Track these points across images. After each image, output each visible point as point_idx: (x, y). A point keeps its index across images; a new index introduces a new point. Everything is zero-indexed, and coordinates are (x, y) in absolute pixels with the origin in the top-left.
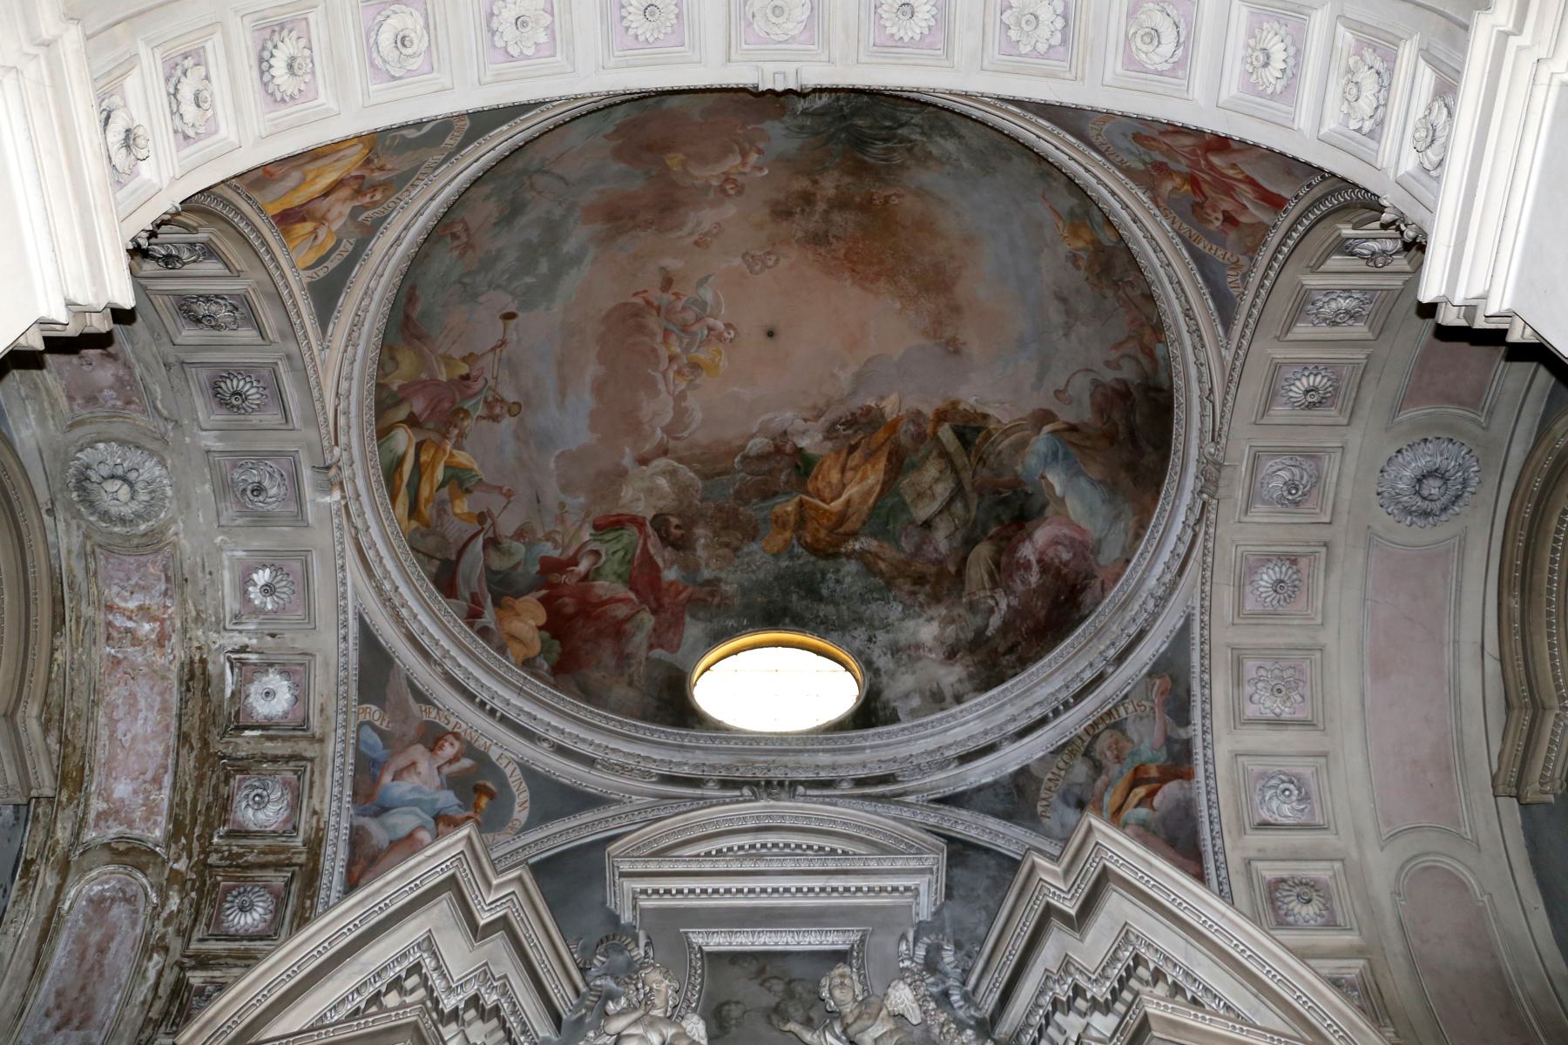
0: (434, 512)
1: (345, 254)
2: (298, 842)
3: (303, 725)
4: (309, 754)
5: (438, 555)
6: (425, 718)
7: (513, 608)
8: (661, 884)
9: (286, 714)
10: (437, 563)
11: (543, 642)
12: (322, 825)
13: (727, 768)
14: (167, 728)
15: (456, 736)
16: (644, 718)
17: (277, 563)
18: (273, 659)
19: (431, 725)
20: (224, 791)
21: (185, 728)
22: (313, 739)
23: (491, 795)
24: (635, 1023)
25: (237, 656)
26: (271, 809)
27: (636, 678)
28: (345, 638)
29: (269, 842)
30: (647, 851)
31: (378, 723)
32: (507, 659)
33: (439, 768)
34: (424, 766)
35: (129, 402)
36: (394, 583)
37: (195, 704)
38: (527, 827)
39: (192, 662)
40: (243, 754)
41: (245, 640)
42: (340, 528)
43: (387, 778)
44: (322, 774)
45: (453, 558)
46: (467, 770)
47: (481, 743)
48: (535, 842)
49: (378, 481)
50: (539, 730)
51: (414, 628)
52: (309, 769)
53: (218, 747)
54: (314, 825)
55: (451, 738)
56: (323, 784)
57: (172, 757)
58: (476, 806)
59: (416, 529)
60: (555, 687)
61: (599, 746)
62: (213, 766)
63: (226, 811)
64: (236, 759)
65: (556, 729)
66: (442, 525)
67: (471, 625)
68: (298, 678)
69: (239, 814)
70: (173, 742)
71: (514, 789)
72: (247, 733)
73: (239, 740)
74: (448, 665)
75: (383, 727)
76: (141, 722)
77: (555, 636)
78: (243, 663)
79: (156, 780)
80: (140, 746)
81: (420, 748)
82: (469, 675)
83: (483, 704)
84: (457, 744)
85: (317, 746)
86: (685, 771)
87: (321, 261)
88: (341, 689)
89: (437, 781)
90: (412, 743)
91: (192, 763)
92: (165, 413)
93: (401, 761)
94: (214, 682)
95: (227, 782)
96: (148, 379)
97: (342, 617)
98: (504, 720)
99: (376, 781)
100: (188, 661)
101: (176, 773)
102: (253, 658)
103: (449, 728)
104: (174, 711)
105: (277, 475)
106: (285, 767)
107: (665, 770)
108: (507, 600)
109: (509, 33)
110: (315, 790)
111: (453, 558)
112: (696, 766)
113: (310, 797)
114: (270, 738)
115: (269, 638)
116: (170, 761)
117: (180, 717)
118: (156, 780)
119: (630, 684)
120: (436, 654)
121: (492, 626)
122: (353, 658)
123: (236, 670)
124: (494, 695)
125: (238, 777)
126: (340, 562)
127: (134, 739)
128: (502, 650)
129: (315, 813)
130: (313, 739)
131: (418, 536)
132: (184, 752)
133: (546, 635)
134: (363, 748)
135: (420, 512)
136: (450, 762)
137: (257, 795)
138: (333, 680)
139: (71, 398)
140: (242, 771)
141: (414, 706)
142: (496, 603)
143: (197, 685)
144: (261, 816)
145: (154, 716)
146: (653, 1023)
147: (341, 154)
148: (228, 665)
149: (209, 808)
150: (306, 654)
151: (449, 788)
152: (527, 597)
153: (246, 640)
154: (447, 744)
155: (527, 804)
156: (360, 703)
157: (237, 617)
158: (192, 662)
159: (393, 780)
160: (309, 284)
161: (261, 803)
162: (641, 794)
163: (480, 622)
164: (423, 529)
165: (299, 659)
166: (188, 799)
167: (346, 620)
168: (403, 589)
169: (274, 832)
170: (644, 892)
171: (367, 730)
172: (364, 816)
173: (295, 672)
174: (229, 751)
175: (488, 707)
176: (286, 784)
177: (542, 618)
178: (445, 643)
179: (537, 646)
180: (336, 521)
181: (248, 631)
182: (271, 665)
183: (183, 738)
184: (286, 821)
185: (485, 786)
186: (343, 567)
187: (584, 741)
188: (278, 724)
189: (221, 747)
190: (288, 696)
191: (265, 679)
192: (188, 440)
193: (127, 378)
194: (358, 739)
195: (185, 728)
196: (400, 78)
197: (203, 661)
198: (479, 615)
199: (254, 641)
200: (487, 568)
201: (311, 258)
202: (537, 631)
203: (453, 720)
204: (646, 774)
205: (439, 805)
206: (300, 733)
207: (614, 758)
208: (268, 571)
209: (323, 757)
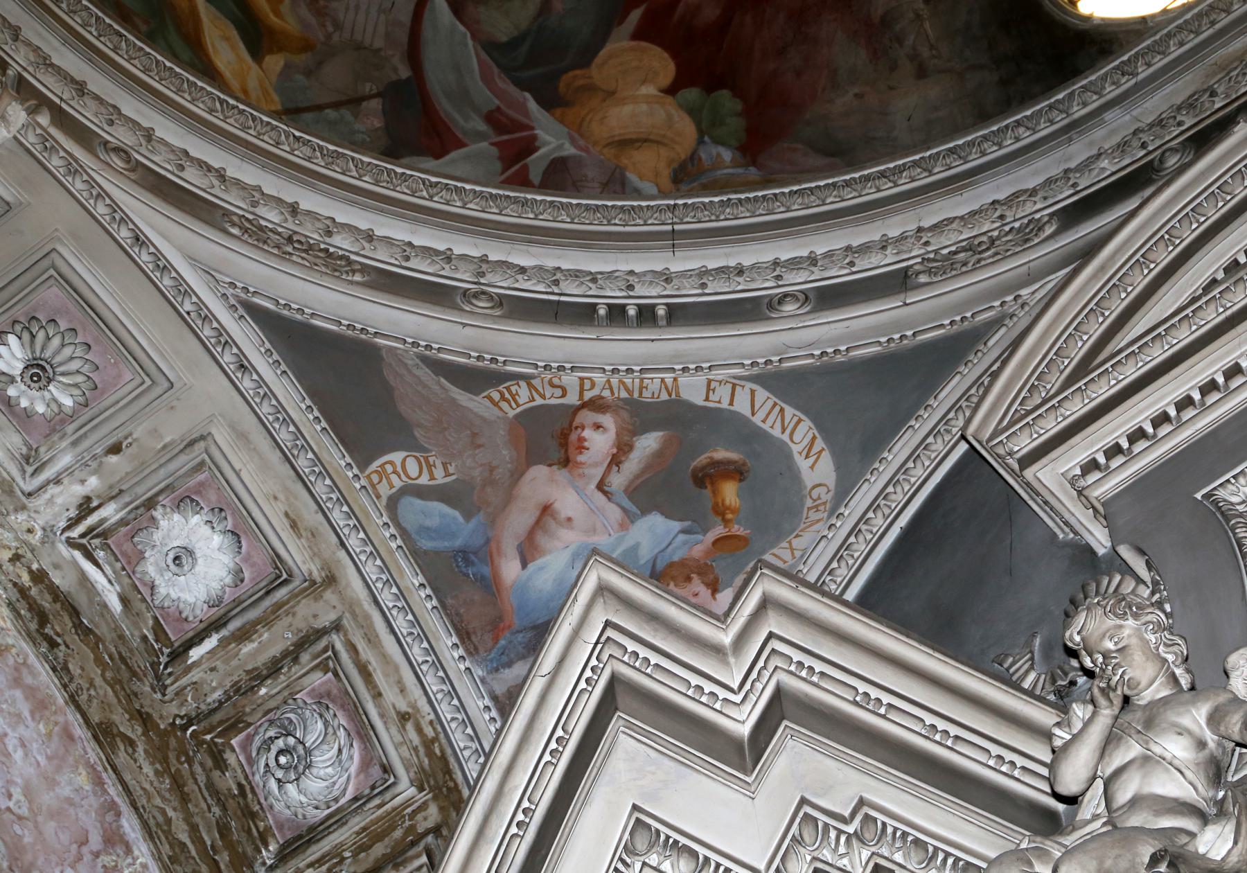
0: (304, 11)
2: (406, 791)
3: (280, 575)
4: (325, 620)
5: (368, 88)
6: (511, 413)
7: (591, 89)
8: (1114, 428)
9: (238, 575)
10: (375, 104)
11: (693, 112)
12: (429, 732)
13: (1190, 105)
14: (69, 736)
15: (596, 405)
16: (983, 117)
17: (19, 312)
18: (144, 491)
19: (533, 417)
20: (228, 782)
21: (96, 718)
22: (313, 588)
23: (737, 472)
24: (1110, 742)
25: (81, 529)
26: (323, 760)
27: (925, 52)
28: (244, 366)
29: (356, 823)
30: (1055, 380)
31: (424, 480)
32: (639, 195)
33: (601, 487)
34: (568, 501)
36: (280, 201)
37: (81, 661)
38: (844, 491)
39: (23, 591)
40: (217, 695)
41: (73, 492)
42: (74, 168)
43: (510, 569)
44: (372, 639)
45: (405, 73)
46: (659, 455)
47: (654, 388)
48: (873, 506)
49: (104, 30)
50: (764, 286)
51: (383, 258)
52: (339, 646)
53: (168, 712)
54: (416, 740)
55: (587, 417)
56: (385, 658)
57: (109, 778)
58: (720, 511)
59: (287, 66)
60: (766, 183)
61: (902, 238)
62: (182, 751)
63: (253, 816)
64: (213, 711)
65: (794, 264)
66: (338, 26)
67: (521, 181)
68: (213, 496)
69: (279, 807)
70: (93, 753)
71: (776, 432)
72: (195, 654)
73: (195, 675)
74: (500, 283)
75: (440, 478)
76: (18, 755)
77: (712, 84)
78: (102, 533)
79: (114, 839)
80: (47, 799)
81: (539, 472)
82: (554, 276)
83: (617, 314)
84: (607, 420)
85: (329, 595)
86: (1109, 169)
88: (303, 463)
89: (613, 513)
90: (517, 475)
91: (148, 769)
93: (518, 521)
94: (82, 601)
95: (220, 764)
97: (207, 332)
98: (679, 315)
99: (491, 586)
100: (14, 595)
101: (134, 804)
102: (110, 513)
103: (572, 399)
104: (60, 698)
106: (297, 671)
107: (1065, 197)
108: (569, 81)
110: (379, 678)
111: (405, 73)
112: (1123, 147)
113: (378, 695)
114: (243, 635)
115: (113, 459)
116: (114, 791)
117: (73, 700)
118: (114, 839)
119: (922, 73)
120: (463, 278)
121: (569, 150)
122: (288, 392)
123: (100, 555)
124: (629, 281)
125: (234, 742)
126: (124, 234)
127: (28, 792)
128: (616, 184)
129: (404, 717)
130: (313, 588)
131: (300, 78)
132: (122, 758)
133: (691, 94)
134: (426, 544)
135: (271, 32)
136: (616, 461)
137: (281, 752)
138: (275, 457)
140: (235, 725)
141: (476, 404)
142: (550, 102)
143: (61, 625)
144: (315, 785)
145: (33, 730)
146: (1152, 717)
148: (78, 555)
149: (224, 830)
150: (191, 444)
151: (645, 511)
152: (609, 48)
153: (79, 491)
154: (587, 433)
155: (820, 444)
156: (363, 464)
157: (30, 460)
158: (23, 591)
159: (524, 565)
161: (301, 765)
162: (1031, 278)
163: (536, 163)
164: (302, 59)
165: (185, 462)
166: (184, 837)
167: (221, 331)
168: (309, 200)
169: (355, 799)
170: (1091, 466)
171: (412, 509)
172: (509, 664)
173: (201, 488)
174: (190, 706)
175: (632, 312)
176: (322, 700)
177: (663, 66)
178: (465, 246)
179: (686, 127)
180: (55, 162)
181: (69, 471)
182: (150, 504)
183: (104, 734)
184: (365, 765)
185: (715, 464)
186: (139, 240)
187: (865, 249)
188: (237, 602)
189: (173, 709)
190: (217, 539)
191: (157, 536)
194: (404, 533)
195: (96, 718)
197: (39, 577)
198: (529, 146)
199: (93, 482)
200: (491, 47)
202: (669, 99)
203: (570, 380)
204: (1028, 233)
205: (645, 554)
206: (282, 593)
207: (947, 242)
208: (12, 339)
209: (352, 606)
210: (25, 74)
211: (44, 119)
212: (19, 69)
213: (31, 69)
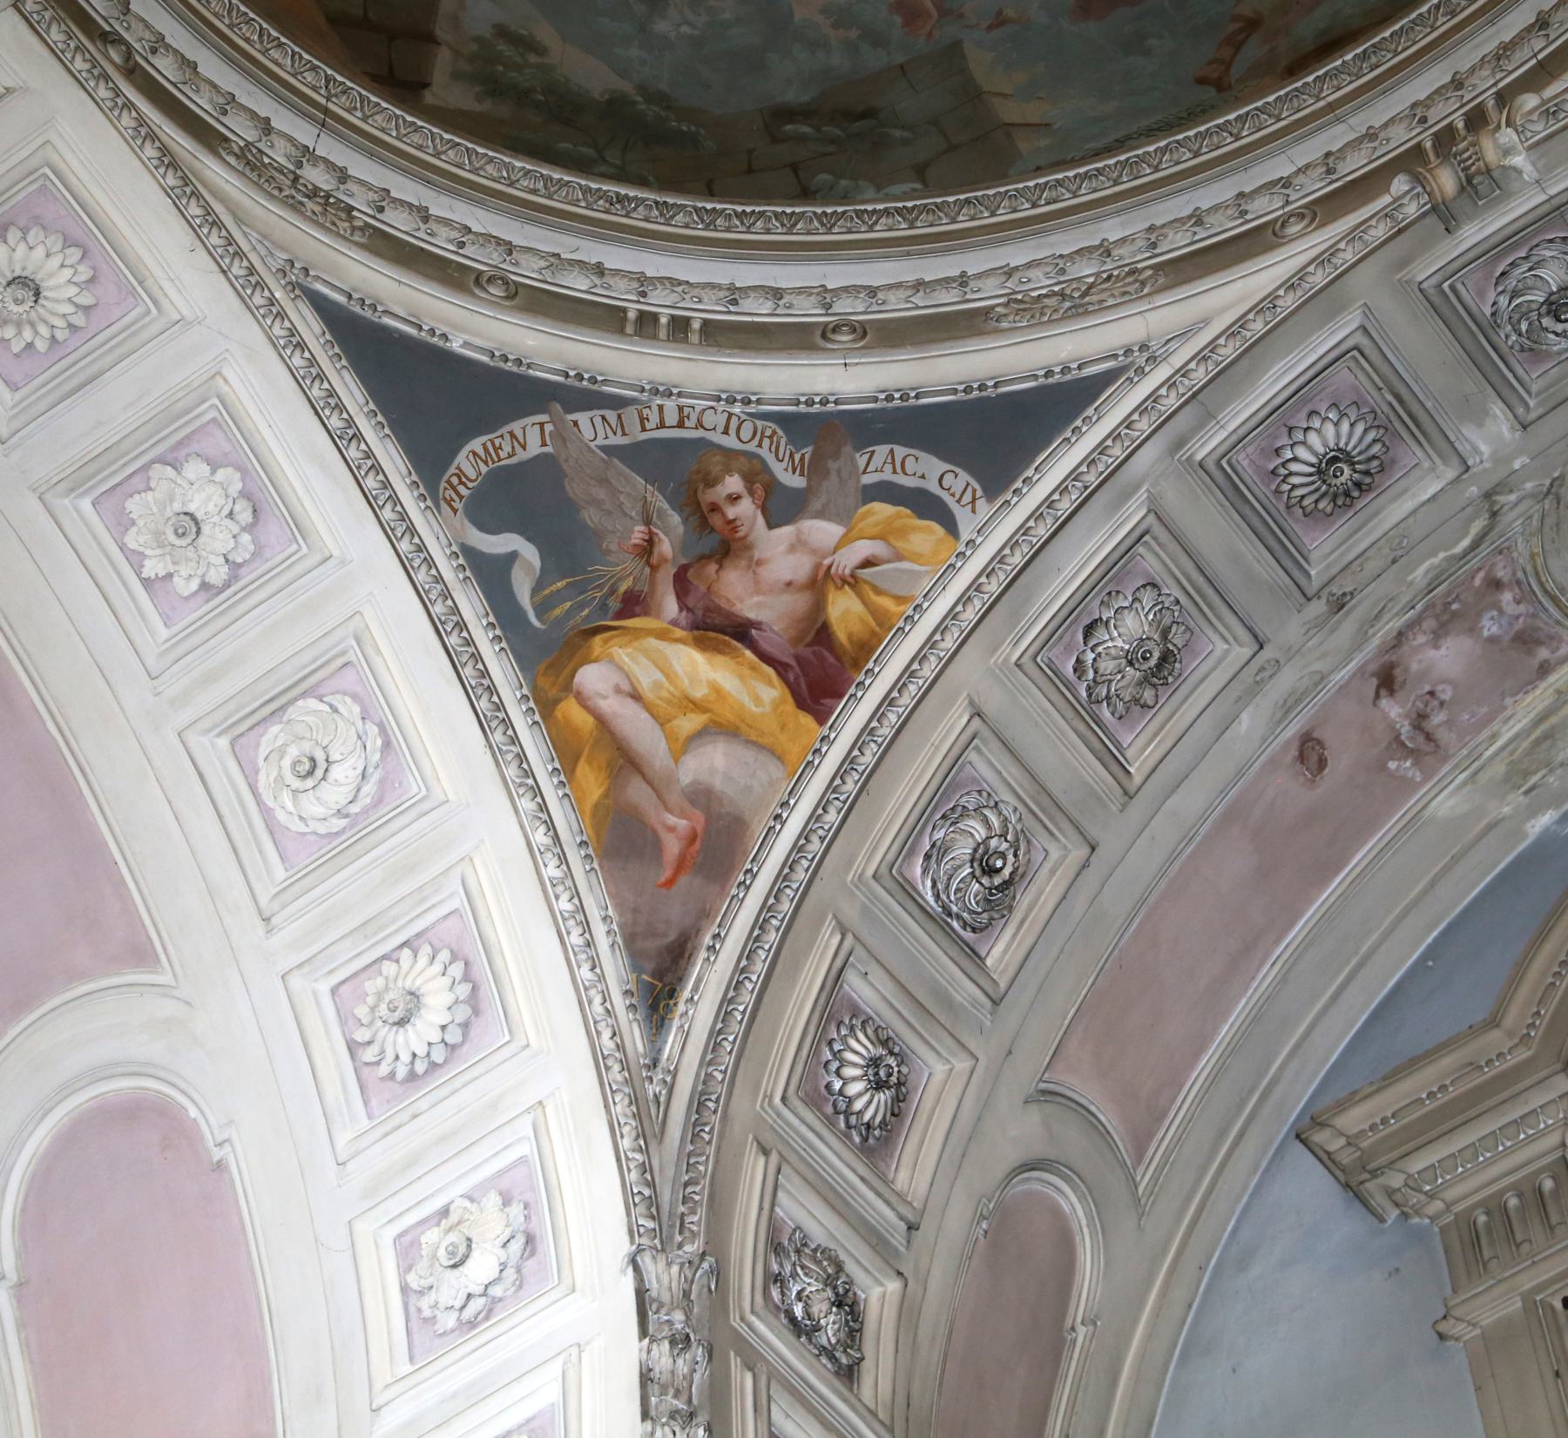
1: (900, 451)
35: (1496, 585)
87: (928, 506)
92: (1477, 527)
96: (1405, 599)
105: (1511, 283)
109: (218, 538)
139: (1544, 670)
147: (612, 705)
160: (991, 492)
192: (1517, 465)
193: (1429, 624)
196: (382, 727)
201: (925, 536)
210: (1501, 85)
211: (1530, 101)
212: (1494, 90)
213: (1498, 76)
